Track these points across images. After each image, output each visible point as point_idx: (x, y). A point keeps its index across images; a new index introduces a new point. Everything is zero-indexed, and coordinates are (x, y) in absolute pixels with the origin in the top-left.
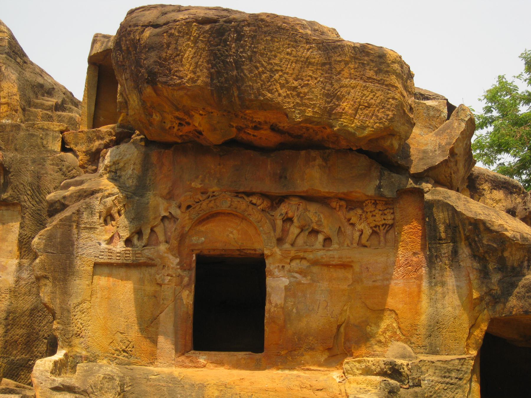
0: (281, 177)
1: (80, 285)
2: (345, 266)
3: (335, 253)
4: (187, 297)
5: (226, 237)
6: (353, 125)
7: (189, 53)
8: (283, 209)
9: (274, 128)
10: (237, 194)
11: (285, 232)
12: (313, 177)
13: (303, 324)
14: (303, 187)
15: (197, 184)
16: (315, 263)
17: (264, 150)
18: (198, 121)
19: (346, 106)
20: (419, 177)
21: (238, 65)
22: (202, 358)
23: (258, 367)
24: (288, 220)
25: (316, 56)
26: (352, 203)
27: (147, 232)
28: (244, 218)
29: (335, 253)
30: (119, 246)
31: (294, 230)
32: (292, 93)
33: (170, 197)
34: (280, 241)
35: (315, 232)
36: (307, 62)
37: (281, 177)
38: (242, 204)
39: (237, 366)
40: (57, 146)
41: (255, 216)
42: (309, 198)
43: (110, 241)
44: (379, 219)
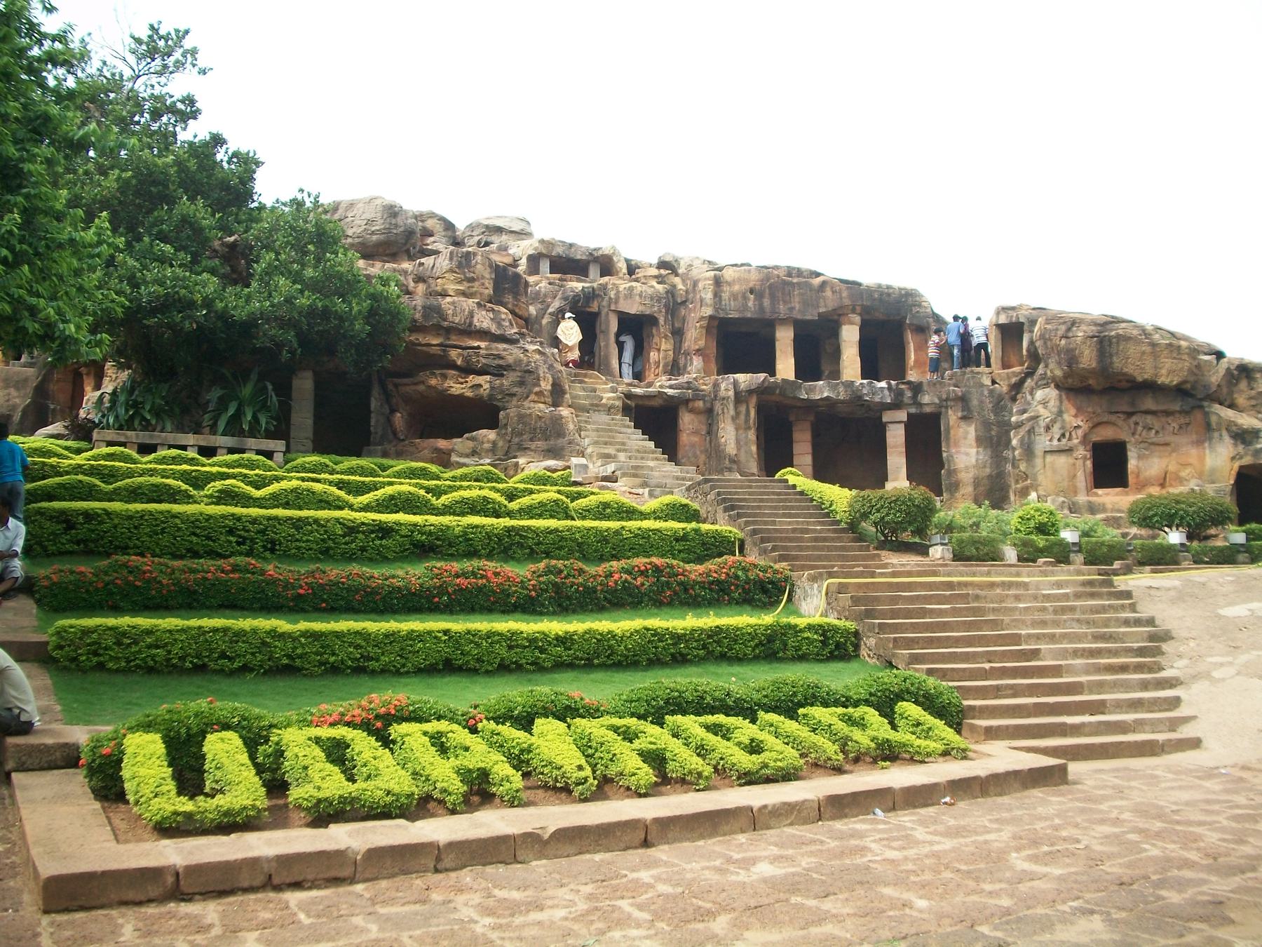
0: (1133, 404)
1: (1038, 461)
2: (1167, 444)
3: (1161, 438)
4: (1089, 464)
5: (1106, 434)
6: (1167, 381)
7: (1087, 352)
8: (1134, 418)
9: (1128, 381)
10: (1111, 413)
11: (1135, 430)
12: (1149, 403)
13: (1147, 474)
14: (1144, 408)
15: (1090, 409)
16: (1153, 444)
17: (1123, 390)
18: (1091, 382)
19: (1164, 371)
20: (1201, 400)
21: (1111, 356)
22: (1100, 491)
23: (1127, 494)
24: (1136, 424)
25: (1148, 349)
26: (1168, 413)
27: (1067, 435)
28: (1114, 424)
29: (1161, 438)
30: (1055, 442)
31: (1140, 428)
32: (1135, 364)
33: (1076, 416)
34: (1133, 434)
35: (1151, 429)
36: (1144, 353)
37: (1133, 404)
38: (1113, 418)
39: (1117, 494)
40: (988, 382)
41: (1120, 423)
42: (1147, 412)
43: (1051, 440)
44: (1182, 421)
